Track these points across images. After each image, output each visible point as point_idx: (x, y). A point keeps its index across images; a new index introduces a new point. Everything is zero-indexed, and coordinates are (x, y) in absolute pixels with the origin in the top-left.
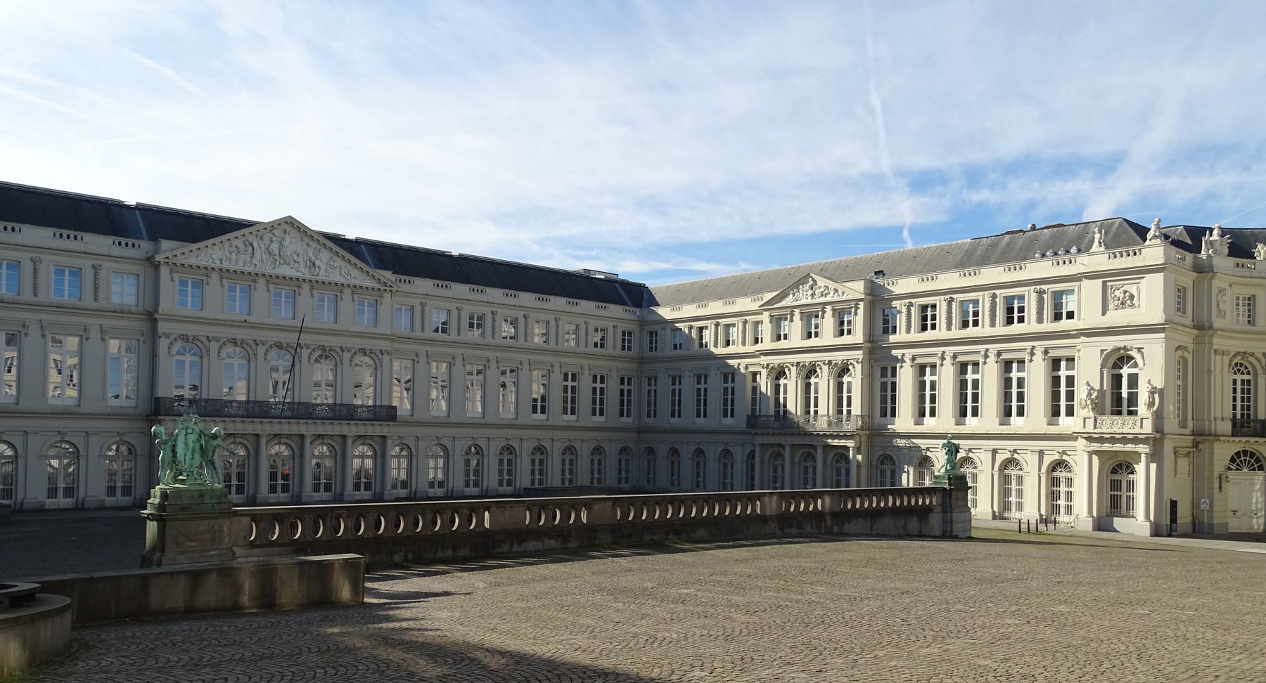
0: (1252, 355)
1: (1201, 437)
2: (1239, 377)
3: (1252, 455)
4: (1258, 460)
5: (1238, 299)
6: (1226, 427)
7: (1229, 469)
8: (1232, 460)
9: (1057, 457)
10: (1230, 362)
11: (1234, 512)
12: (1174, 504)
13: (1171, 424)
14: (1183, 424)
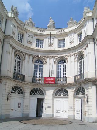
0: (22, 52)
2: (17, 60)
3: (19, 88)
4: (21, 90)
5: (19, 33)
6: (12, 75)
8: (13, 89)
10: (15, 53)
11: (12, 110)
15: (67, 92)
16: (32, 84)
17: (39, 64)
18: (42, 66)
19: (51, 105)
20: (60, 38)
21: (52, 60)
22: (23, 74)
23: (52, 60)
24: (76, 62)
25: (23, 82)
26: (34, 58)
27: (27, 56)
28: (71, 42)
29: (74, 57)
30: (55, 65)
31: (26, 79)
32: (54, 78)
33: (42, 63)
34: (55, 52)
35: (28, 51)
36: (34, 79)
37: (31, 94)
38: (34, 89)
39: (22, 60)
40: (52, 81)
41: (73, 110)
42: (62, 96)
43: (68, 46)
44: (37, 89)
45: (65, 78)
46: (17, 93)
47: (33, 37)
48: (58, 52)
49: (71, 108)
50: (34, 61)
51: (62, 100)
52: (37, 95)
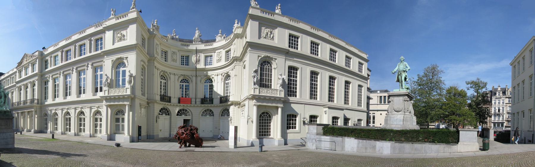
0: (167, 72)
1: (150, 103)
3: (166, 109)
4: (168, 112)
6: (158, 98)
7: (160, 114)
8: (160, 111)
12: (140, 128)
13: (138, 93)
14: (143, 94)
15: (213, 113)
17: (184, 84)
18: (188, 86)
22: (169, 95)
25: (169, 104)
26: (179, 77)
28: (219, 60)
29: (220, 77)
38: (180, 110)
42: (208, 116)
43: (215, 65)
44: (183, 110)
50: (180, 80)
52: (183, 116)
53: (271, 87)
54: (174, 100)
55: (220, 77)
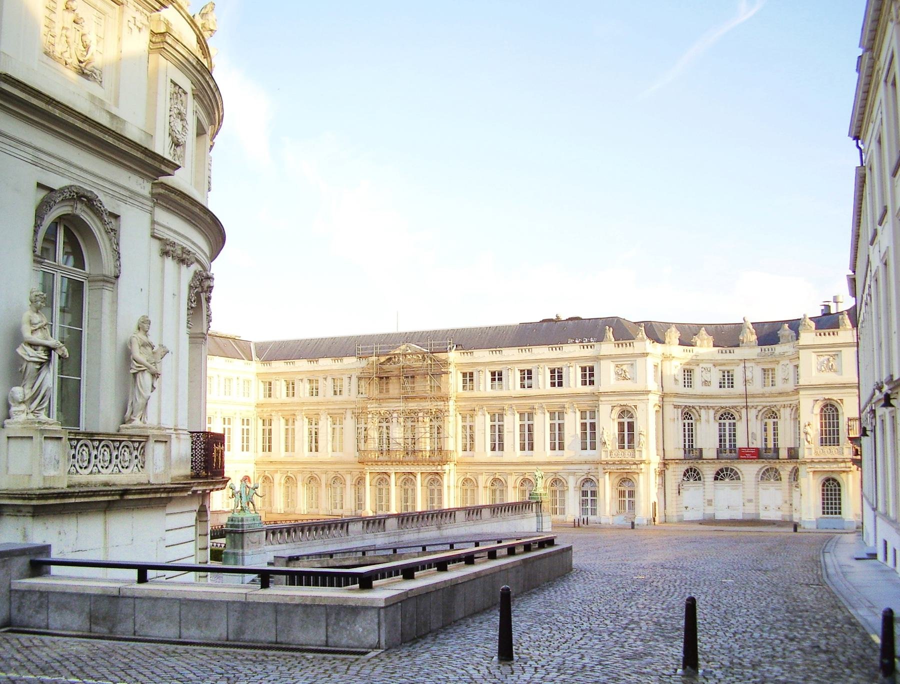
0: (693, 407)
2: (686, 421)
3: (695, 470)
4: (698, 474)
6: (681, 455)
8: (685, 475)
9: (585, 477)
16: (716, 461)
17: (727, 422)
18: (734, 424)
19: (753, 498)
20: (766, 367)
21: (753, 413)
23: (753, 413)
24: (792, 422)
27: (703, 412)
29: (788, 410)
30: (759, 422)
31: (705, 455)
32: (757, 449)
33: (734, 419)
34: (753, 396)
35: (703, 401)
36: (720, 451)
37: (716, 479)
38: (722, 470)
39: (696, 420)
40: (752, 454)
41: (787, 505)
43: (780, 386)
44: (727, 469)
45: (776, 450)
46: (691, 480)
47: (713, 369)
48: (763, 395)
49: (786, 502)
50: (718, 416)
51: (772, 489)
52: (727, 480)
53: (838, 442)
54: (710, 452)
55: (788, 410)
